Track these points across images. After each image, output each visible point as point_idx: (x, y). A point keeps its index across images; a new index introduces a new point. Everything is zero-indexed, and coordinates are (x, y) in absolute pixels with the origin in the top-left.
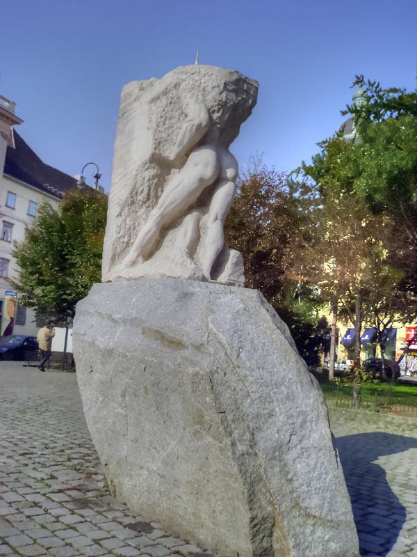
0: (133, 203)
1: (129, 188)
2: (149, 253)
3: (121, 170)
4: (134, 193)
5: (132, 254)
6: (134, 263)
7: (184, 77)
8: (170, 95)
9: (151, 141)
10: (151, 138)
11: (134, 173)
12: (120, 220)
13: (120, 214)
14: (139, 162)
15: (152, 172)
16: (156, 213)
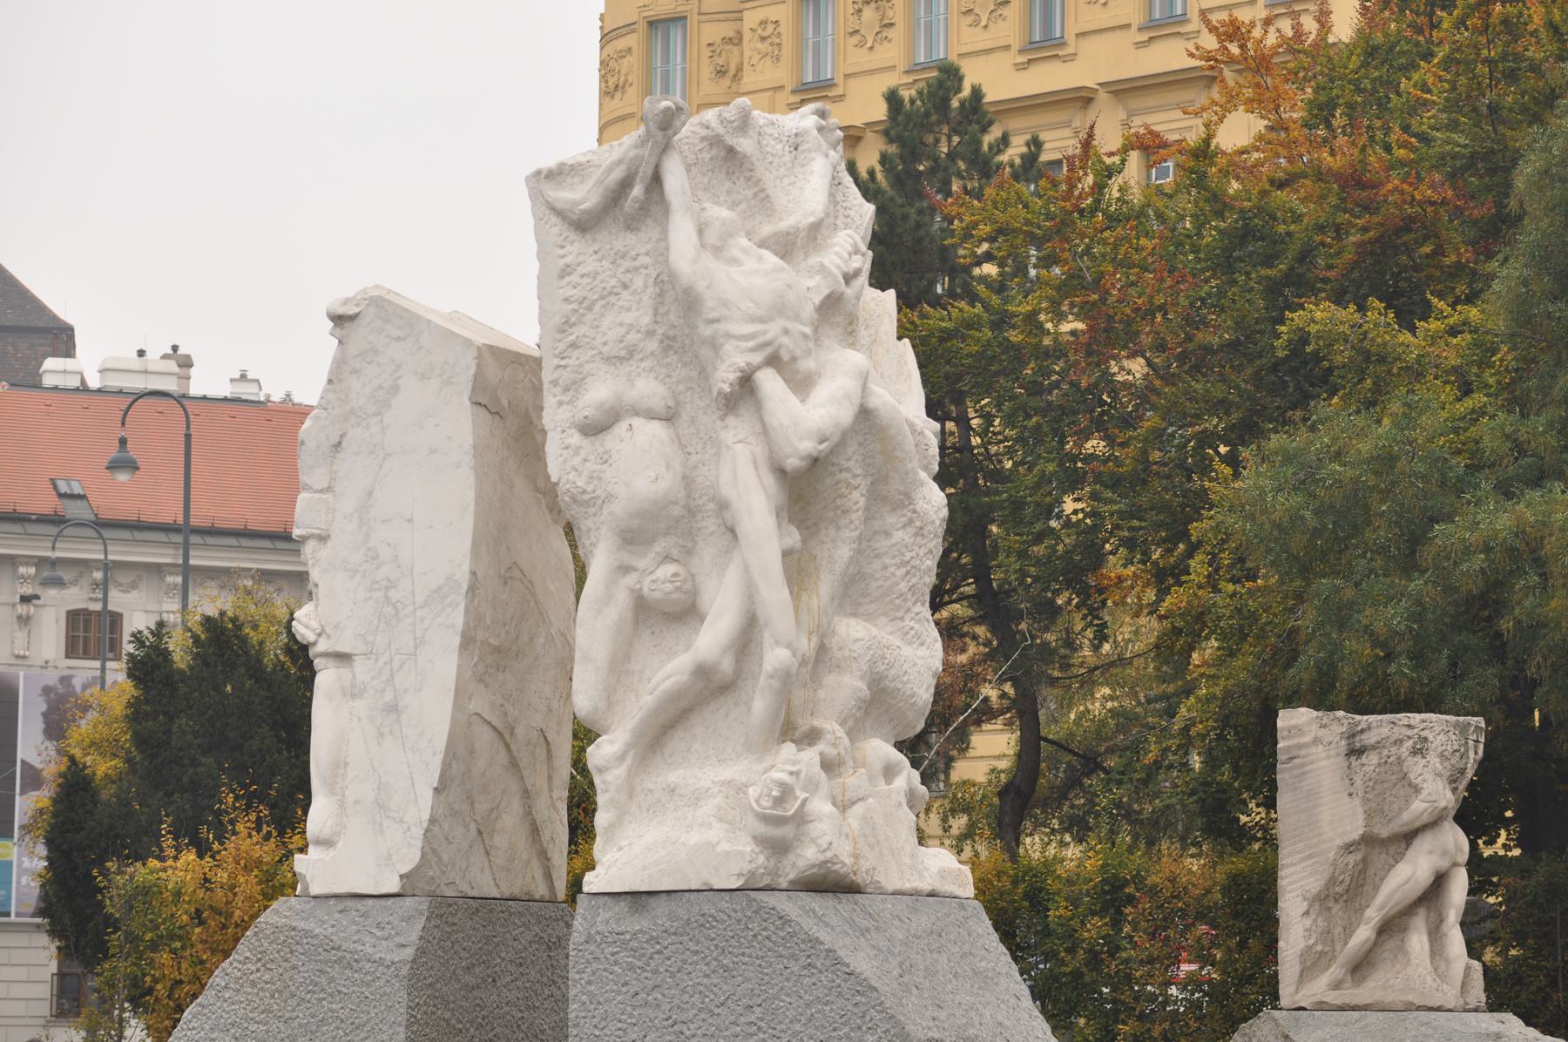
0: (1327, 896)
1: (1327, 875)
2: (1361, 967)
3: (1300, 846)
4: (1332, 881)
5: (1335, 971)
6: (1337, 986)
7: (1409, 733)
8: (1385, 752)
9: (1361, 817)
10: (1360, 810)
11: (1331, 856)
12: (1308, 922)
13: (1307, 913)
14: (1339, 842)
15: (1359, 856)
16: (1373, 915)
